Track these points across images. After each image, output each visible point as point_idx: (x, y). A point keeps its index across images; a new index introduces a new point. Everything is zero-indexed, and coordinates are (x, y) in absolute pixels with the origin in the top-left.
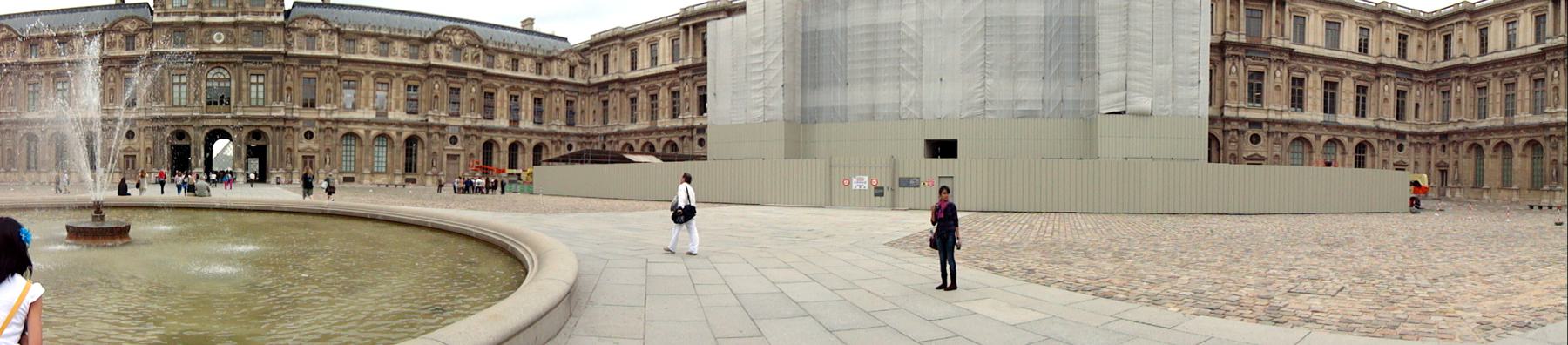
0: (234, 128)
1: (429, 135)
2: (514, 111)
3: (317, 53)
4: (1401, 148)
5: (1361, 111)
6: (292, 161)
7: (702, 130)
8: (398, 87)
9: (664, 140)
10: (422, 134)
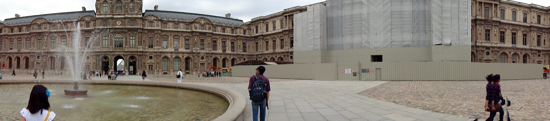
0: (124, 55)
1: (193, 56)
2: (224, 47)
3: (153, 28)
4: (539, 56)
5: (525, 43)
6: (145, 67)
7: (292, 53)
8: (182, 40)
9: (278, 57)
10: (191, 56)
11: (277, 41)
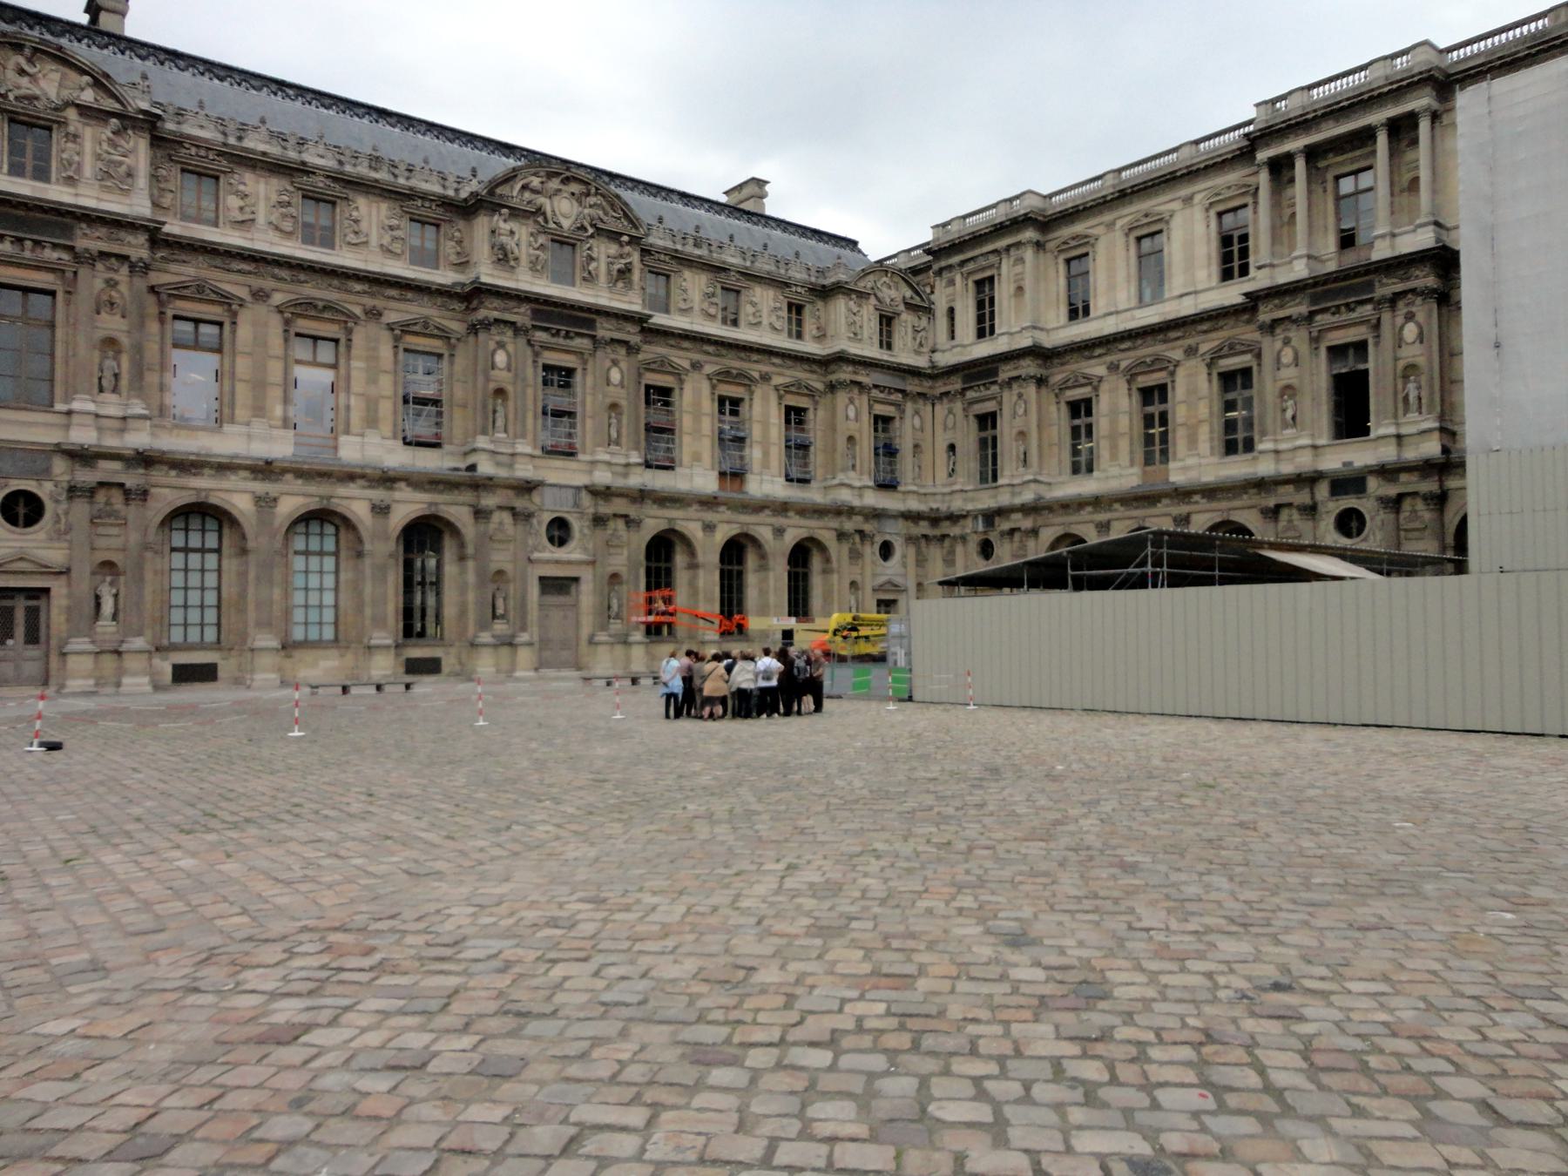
1: (480, 514)
3: (57, 193)
10: (456, 510)
11: (1179, 392)
